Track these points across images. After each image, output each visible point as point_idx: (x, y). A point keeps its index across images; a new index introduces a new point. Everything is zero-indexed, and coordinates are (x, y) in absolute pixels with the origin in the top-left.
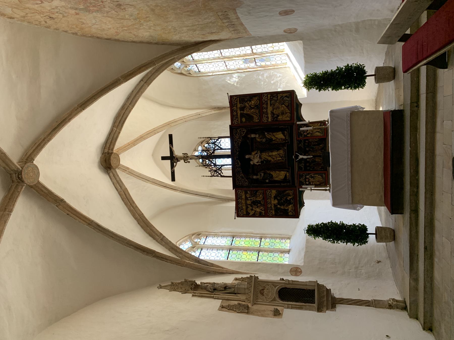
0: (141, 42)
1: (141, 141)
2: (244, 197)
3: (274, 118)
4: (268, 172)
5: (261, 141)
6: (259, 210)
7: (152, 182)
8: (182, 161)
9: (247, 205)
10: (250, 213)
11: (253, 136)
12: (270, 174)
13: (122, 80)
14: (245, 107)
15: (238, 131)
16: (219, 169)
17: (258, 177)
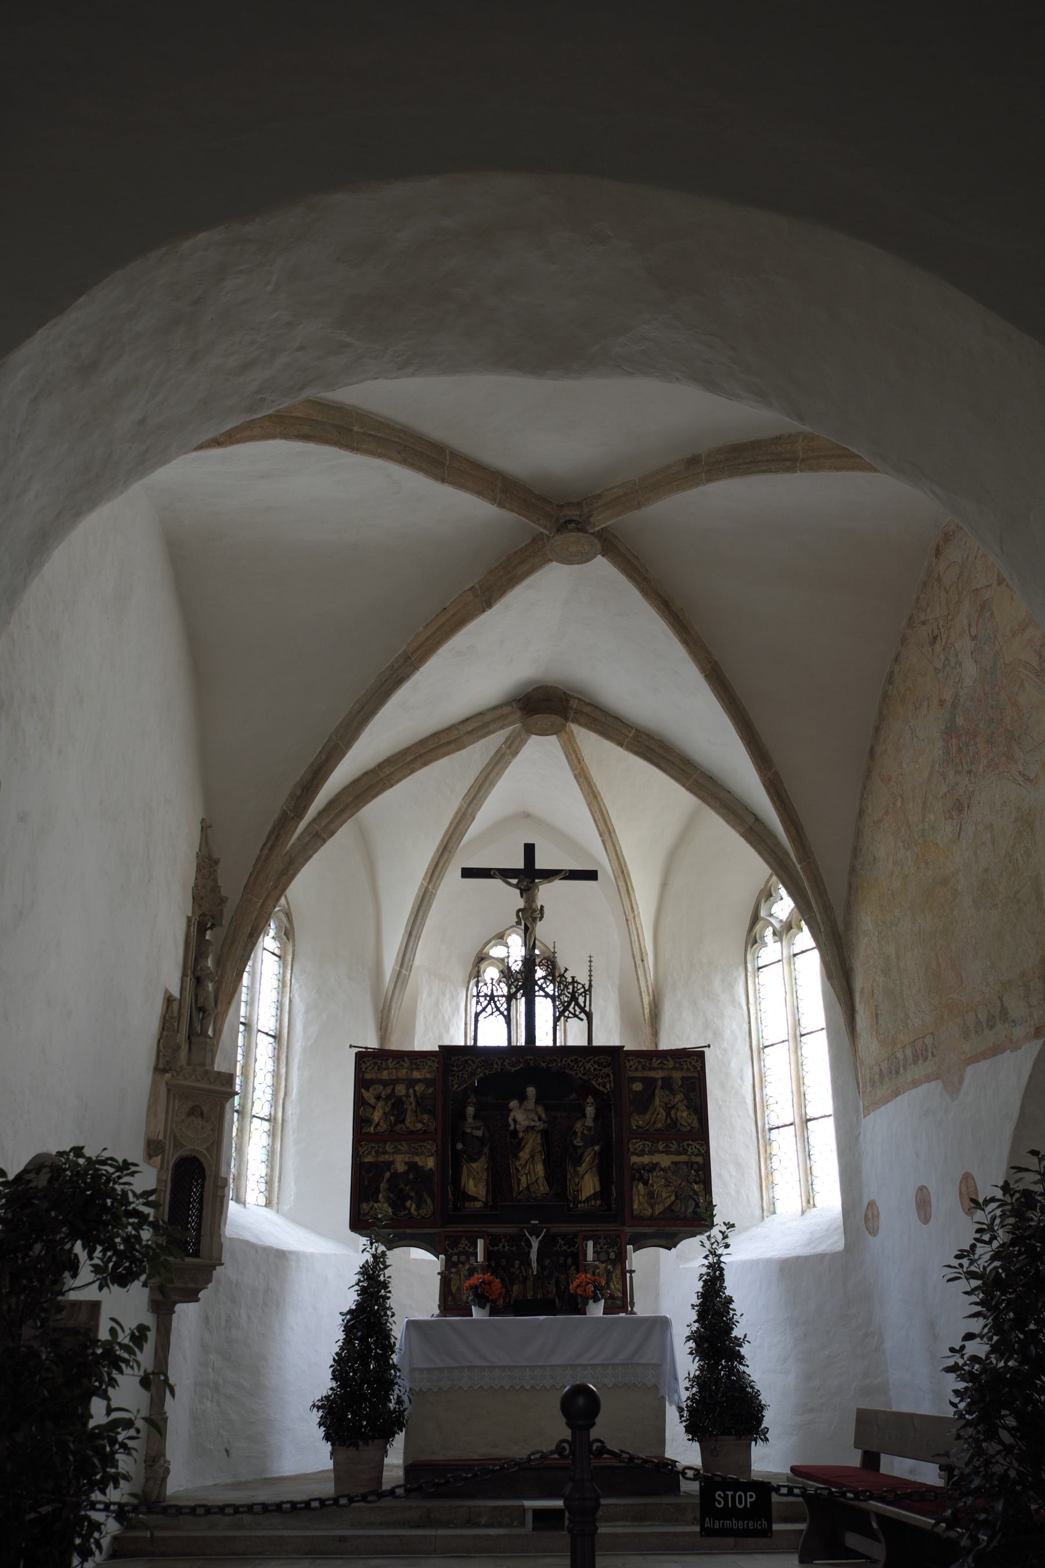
0: (859, 833)
2: (416, 1075)
3: (638, 1171)
4: (486, 1150)
5: (575, 1133)
6: (376, 1119)
7: (464, 814)
8: (521, 903)
10: (367, 1090)
11: (590, 1111)
14: (673, 1092)
15: (606, 1070)
16: (498, 1009)
17: (470, 1120)
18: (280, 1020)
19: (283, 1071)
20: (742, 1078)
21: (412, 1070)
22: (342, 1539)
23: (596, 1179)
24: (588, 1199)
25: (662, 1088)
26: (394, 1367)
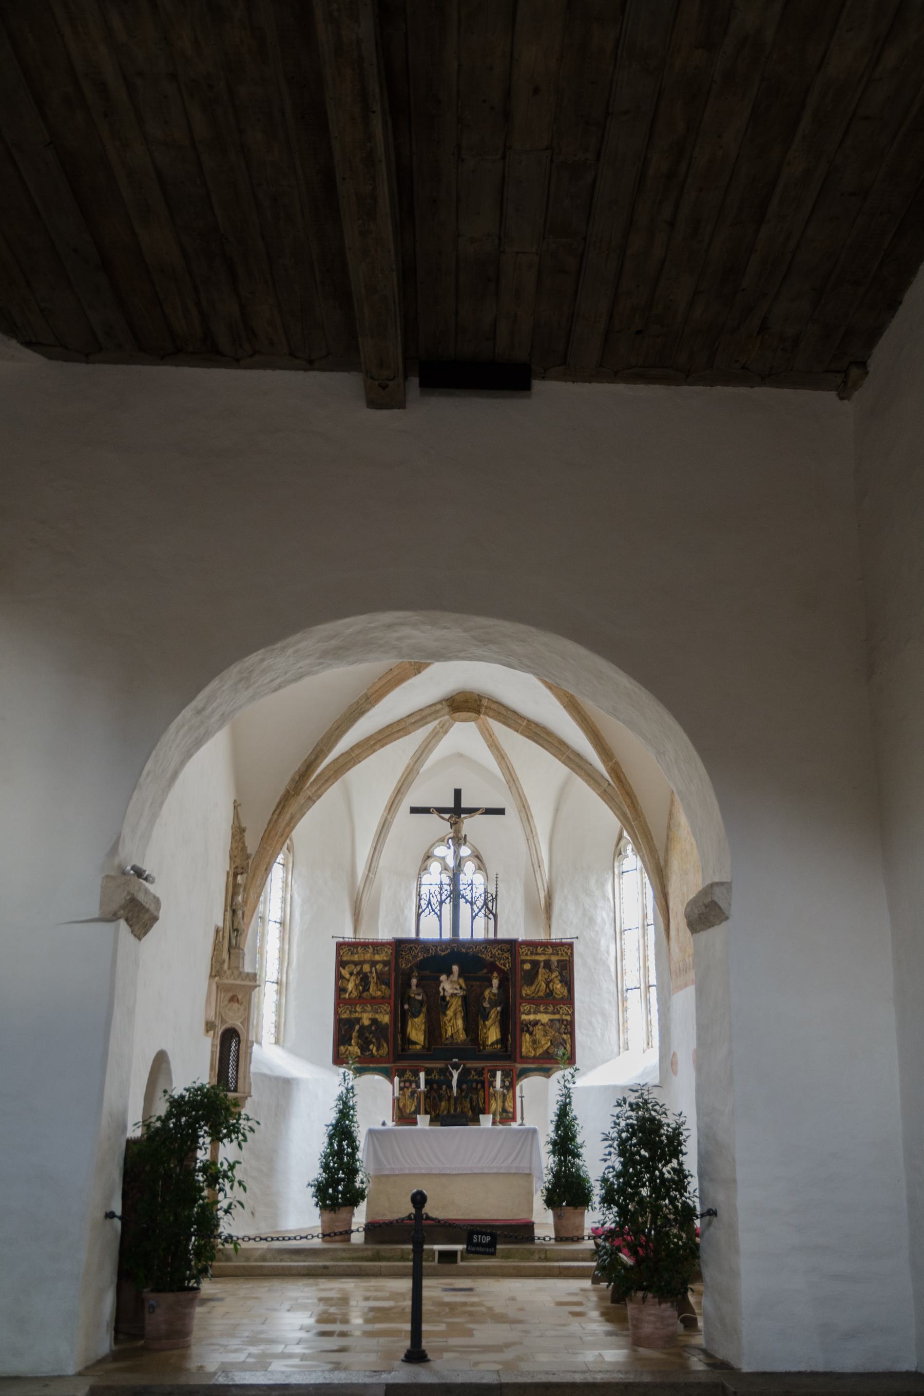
1: (496, 758)
2: (377, 958)
3: (526, 1025)
4: (424, 1009)
5: (485, 998)
7: (412, 769)
9: (361, 963)
10: (344, 968)
11: (495, 982)
12: (419, 1013)
13: (611, 764)
14: (551, 970)
15: (506, 955)
17: (414, 988)
18: (284, 910)
19: (287, 947)
20: (608, 953)
21: (374, 955)
22: (325, 1267)
23: (498, 1031)
24: (493, 1044)
25: (544, 967)
26: (358, 1160)
